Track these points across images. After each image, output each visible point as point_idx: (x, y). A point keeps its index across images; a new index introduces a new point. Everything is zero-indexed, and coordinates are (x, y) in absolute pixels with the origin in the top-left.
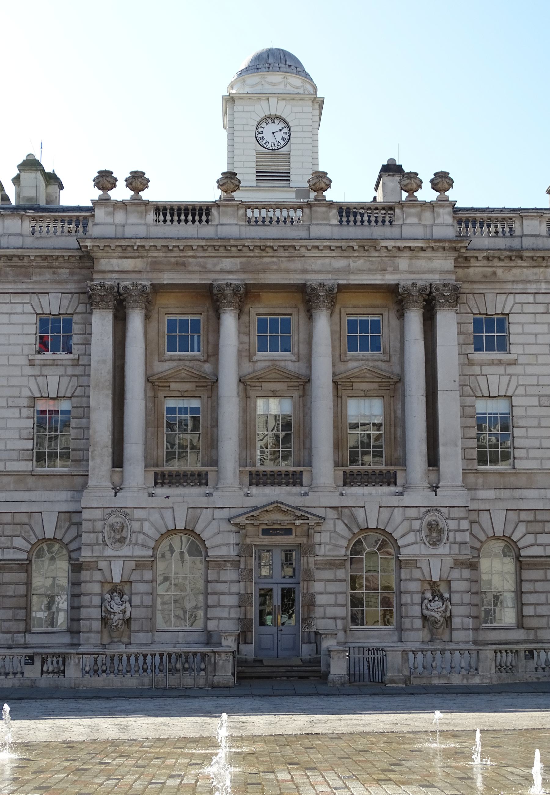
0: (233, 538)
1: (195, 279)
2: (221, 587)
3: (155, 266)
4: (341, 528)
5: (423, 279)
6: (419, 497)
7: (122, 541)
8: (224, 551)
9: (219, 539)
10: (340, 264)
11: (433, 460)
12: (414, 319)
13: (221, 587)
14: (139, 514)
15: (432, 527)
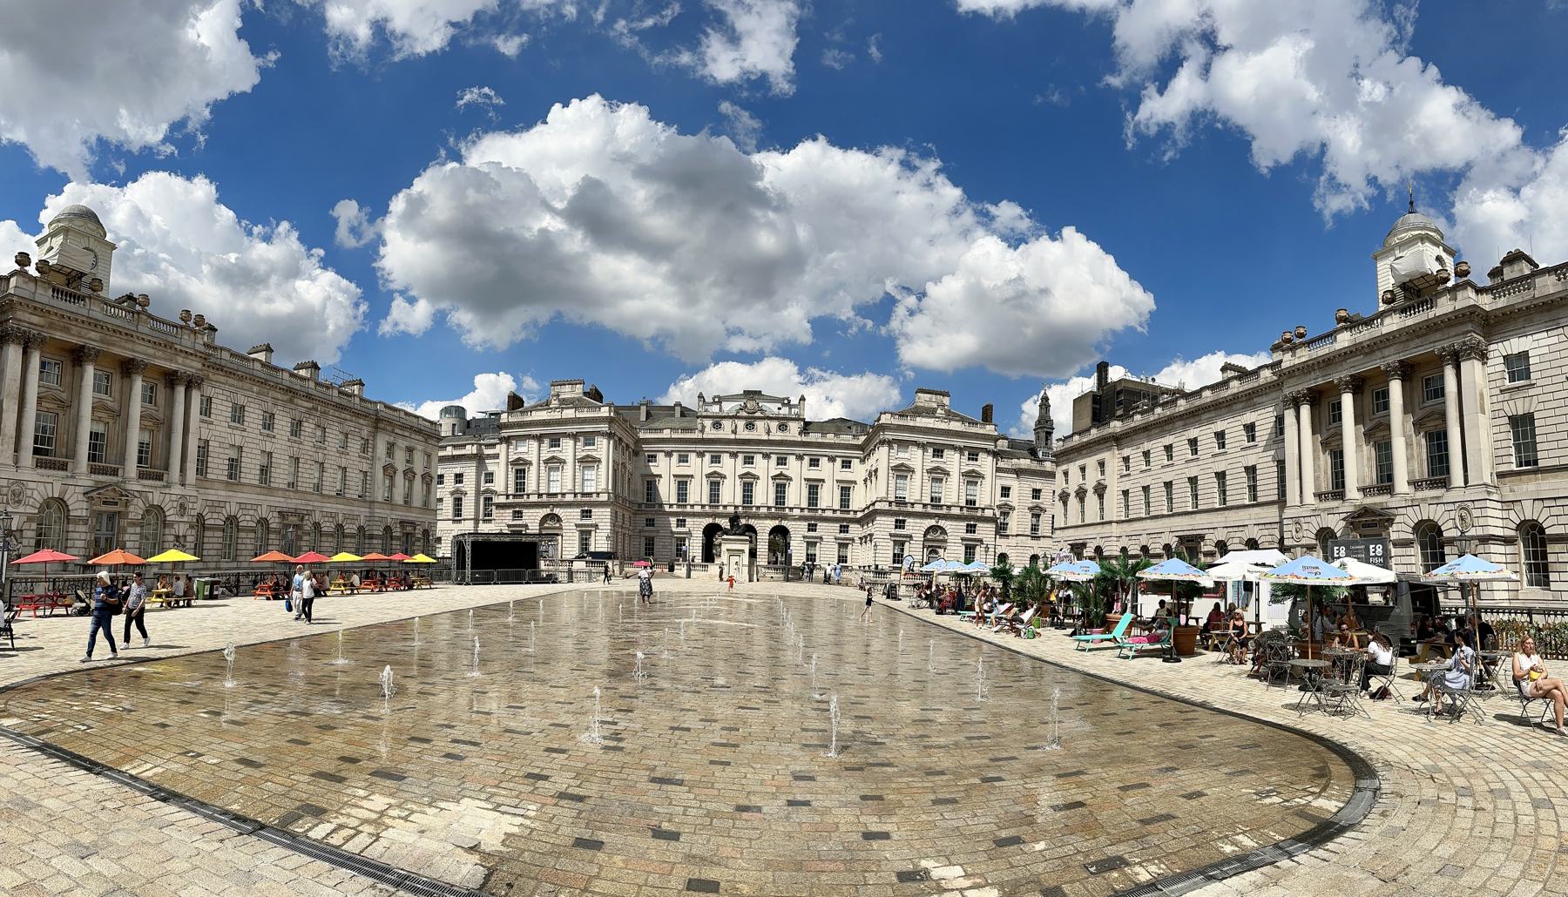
0: (85, 505)
1: (75, 340)
2: (76, 536)
3: (51, 326)
4: (141, 504)
5: (191, 371)
6: (177, 490)
7: (19, 502)
8: (78, 513)
9: (77, 505)
10: (151, 351)
11: (183, 470)
12: (180, 390)
13: (76, 536)
14: (31, 485)
15: (182, 506)
